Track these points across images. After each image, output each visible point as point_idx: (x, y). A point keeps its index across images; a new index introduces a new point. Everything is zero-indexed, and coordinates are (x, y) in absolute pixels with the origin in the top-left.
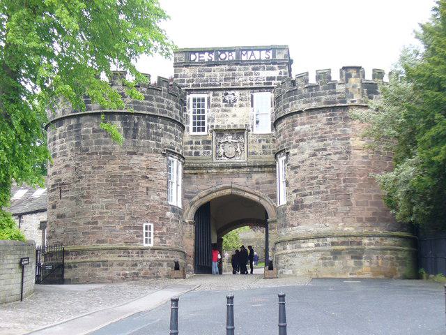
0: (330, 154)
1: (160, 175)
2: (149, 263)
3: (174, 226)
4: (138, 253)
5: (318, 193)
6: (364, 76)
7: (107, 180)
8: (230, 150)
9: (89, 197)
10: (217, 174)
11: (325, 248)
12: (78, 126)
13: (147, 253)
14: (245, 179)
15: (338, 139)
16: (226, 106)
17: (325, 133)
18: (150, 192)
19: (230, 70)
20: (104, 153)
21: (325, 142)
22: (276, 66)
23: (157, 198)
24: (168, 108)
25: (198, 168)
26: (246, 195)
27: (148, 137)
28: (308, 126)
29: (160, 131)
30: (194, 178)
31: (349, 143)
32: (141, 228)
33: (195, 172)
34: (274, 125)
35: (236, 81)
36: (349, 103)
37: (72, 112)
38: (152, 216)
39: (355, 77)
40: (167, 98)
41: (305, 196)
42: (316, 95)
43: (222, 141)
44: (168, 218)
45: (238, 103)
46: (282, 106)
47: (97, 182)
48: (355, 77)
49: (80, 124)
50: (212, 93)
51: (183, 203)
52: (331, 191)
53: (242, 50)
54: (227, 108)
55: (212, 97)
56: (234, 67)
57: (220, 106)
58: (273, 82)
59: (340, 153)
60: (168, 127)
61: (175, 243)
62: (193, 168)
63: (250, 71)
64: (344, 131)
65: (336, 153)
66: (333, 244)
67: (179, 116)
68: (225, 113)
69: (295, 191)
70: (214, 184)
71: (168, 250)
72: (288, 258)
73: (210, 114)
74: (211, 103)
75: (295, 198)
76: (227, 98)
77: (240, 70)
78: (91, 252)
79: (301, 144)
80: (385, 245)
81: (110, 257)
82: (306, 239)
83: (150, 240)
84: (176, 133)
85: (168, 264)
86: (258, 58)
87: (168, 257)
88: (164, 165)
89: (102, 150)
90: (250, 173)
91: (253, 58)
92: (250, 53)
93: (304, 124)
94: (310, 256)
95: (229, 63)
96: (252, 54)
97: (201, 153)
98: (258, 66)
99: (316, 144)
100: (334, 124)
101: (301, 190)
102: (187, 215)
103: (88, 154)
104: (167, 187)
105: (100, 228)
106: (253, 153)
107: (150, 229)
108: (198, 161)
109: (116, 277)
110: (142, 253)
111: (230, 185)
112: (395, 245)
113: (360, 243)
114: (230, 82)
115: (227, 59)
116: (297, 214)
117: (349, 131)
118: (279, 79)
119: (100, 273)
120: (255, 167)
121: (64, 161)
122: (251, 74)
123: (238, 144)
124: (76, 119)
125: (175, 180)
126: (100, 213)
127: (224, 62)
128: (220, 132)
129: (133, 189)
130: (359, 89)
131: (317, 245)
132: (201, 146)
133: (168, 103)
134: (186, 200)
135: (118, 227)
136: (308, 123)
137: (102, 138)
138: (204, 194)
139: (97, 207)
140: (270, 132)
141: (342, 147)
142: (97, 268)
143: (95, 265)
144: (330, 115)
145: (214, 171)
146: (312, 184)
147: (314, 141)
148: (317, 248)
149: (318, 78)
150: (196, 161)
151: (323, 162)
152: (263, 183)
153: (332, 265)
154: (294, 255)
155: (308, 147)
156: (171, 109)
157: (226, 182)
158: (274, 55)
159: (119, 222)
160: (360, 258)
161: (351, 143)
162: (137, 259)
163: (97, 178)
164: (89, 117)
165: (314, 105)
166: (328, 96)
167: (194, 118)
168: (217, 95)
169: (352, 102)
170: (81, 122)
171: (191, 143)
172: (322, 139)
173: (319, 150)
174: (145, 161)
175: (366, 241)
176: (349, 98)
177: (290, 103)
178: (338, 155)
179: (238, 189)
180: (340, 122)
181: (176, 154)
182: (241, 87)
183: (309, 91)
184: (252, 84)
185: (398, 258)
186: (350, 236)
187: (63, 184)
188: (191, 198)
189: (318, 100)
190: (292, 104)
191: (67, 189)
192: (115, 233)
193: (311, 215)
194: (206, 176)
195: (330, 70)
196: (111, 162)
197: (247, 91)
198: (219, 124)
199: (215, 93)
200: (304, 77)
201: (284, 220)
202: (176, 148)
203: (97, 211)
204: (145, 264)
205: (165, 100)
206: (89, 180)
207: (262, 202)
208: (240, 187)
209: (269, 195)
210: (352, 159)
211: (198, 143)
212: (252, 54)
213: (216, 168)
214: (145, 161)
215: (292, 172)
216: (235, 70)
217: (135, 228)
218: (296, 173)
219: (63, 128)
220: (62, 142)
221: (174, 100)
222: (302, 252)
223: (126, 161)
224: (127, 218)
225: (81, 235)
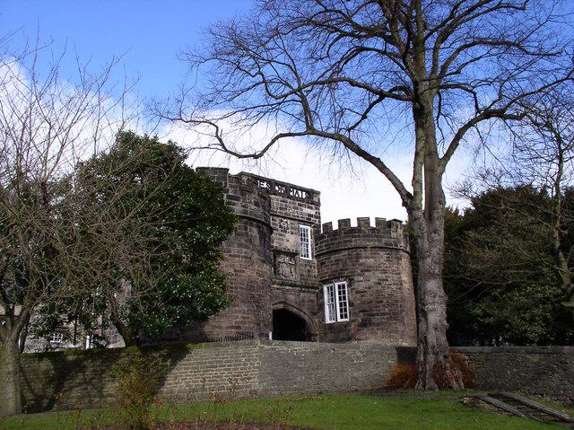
5: (384, 314)
20: (246, 257)
45: (289, 230)
56: (286, 199)
79: (366, 273)
103: (230, 256)
212: (297, 192)
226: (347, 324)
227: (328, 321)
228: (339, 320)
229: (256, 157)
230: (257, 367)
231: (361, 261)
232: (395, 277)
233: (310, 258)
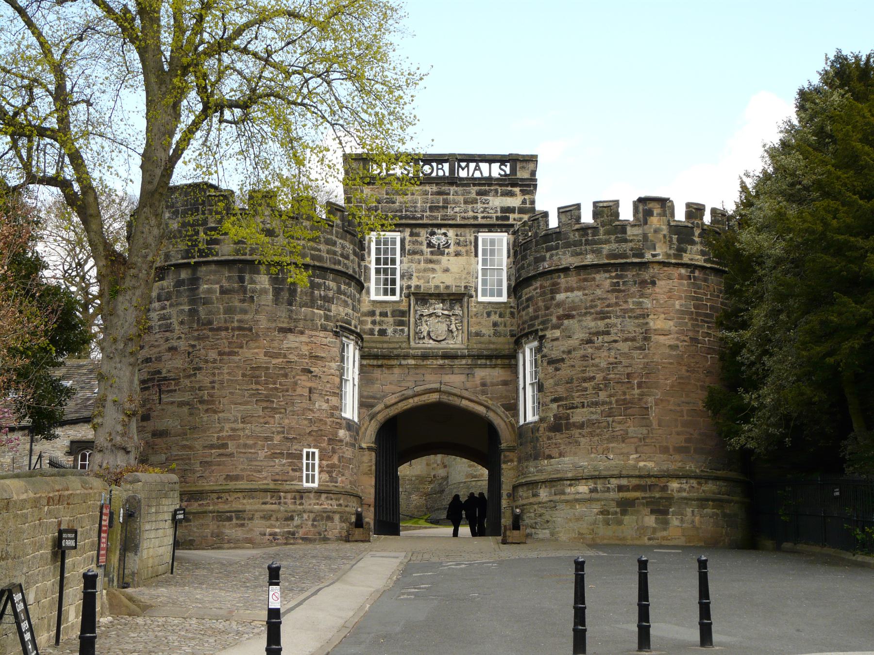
0: (615, 341)
1: (330, 368)
2: (312, 516)
3: (348, 453)
4: (295, 498)
5: (596, 404)
6: (673, 214)
7: (244, 375)
8: (441, 328)
9: (212, 402)
10: (417, 367)
11: (607, 494)
12: (194, 281)
13: (309, 498)
14: (462, 378)
15: (630, 317)
16: (432, 253)
17: (608, 306)
18: (315, 396)
19: (439, 193)
20: (240, 329)
21: (607, 321)
22: (517, 190)
23: (325, 406)
24: (342, 255)
25: (384, 357)
26: (465, 403)
27: (312, 304)
28: (580, 293)
29: (330, 294)
30: (377, 373)
31: (647, 323)
32: (300, 457)
33: (380, 362)
34: (515, 290)
35: (450, 212)
36: (648, 257)
37: (183, 258)
38: (316, 437)
39: (659, 215)
40: (341, 238)
41: (573, 408)
42: (595, 242)
43: (426, 312)
44: (341, 441)
45: (452, 249)
46: (531, 258)
47: (227, 377)
48: (659, 215)
49: (198, 279)
50: (408, 231)
51: (359, 417)
52: (617, 401)
53: (463, 161)
54: (434, 257)
55: (408, 238)
56: (445, 188)
57: (421, 253)
58: (512, 216)
59: (633, 340)
60: (343, 287)
61: (350, 482)
62: (376, 357)
63: (474, 195)
64: (640, 303)
65: (626, 340)
66: (620, 488)
67: (357, 269)
68: (431, 266)
69: (555, 400)
70: (411, 384)
71: (340, 493)
72: (543, 511)
73: (406, 266)
74: (407, 247)
75: (555, 412)
76: (434, 240)
77: (456, 193)
78: (215, 496)
79: (566, 322)
80: (704, 491)
81: (249, 505)
82: (576, 480)
83: (313, 476)
84: (353, 300)
85: (341, 518)
86: (486, 174)
87: (340, 505)
88: (335, 351)
89: (236, 324)
90: (471, 367)
91: (477, 174)
92: (472, 165)
94: (579, 509)
95: (439, 181)
96: (477, 168)
97: (390, 331)
98: (487, 188)
99: (592, 324)
100: (624, 291)
101: (566, 399)
102: (365, 433)
103: (211, 330)
104: (340, 387)
105: (231, 455)
106: (477, 334)
107: (313, 459)
108: (385, 345)
109: (258, 539)
110: (302, 498)
111: (436, 386)
112: (719, 494)
113: (664, 488)
114: (439, 215)
115: (434, 174)
116: (559, 438)
117: (647, 303)
118: (522, 211)
119: (231, 531)
120: (480, 357)
121: (167, 340)
122: (475, 201)
123: (453, 318)
124: (190, 271)
125: (350, 378)
126: (233, 430)
127: (429, 180)
128: (423, 298)
129: (287, 391)
130: (665, 236)
131: (593, 491)
132: (390, 319)
133: (343, 247)
134: (364, 410)
135: (262, 454)
136: (579, 289)
137: (237, 304)
138: (393, 401)
139: (227, 420)
140: (504, 298)
141: (637, 329)
142: (227, 523)
143: (223, 517)
144: (617, 277)
145: (412, 362)
146: (586, 389)
147: (589, 318)
148: (594, 495)
149: (596, 215)
150: (379, 345)
151: (606, 354)
152: (493, 385)
153: (620, 523)
154: (553, 505)
156: (347, 257)
157: (432, 380)
158: (513, 170)
159: (263, 446)
160: (665, 512)
161: (651, 324)
162: (292, 507)
163: (226, 371)
164: (213, 267)
165: (590, 259)
166: (614, 246)
167: (378, 271)
168: (418, 235)
169: (654, 256)
170: (199, 274)
171: (372, 313)
172: (603, 316)
173: (598, 334)
174: (307, 344)
175: (674, 485)
176: (649, 249)
177: (548, 255)
178: (630, 343)
180: (634, 289)
181: (352, 332)
182: (459, 221)
183: (583, 236)
184: (476, 218)
185: (725, 515)
186: (649, 476)
187: (165, 379)
188: (372, 406)
189: (598, 252)
190: (552, 256)
191: (173, 388)
192: (257, 463)
194: (396, 371)
195: (617, 203)
197: (467, 230)
198: (421, 283)
199: (415, 231)
200: (570, 212)
201: (535, 448)
202: (353, 322)
203: (227, 426)
204: (305, 516)
205: (339, 241)
206: (214, 374)
207: (491, 416)
209: (503, 405)
210: (653, 350)
211: (384, 314)
213: (414, 357)
214: (307, 344)
215: (551, 369)
216: (448, 194)
217: (290, 455)
218: (557, 369)
219: (164, 283)
220: (163, 308)
221: (351, 242)
222: (567, 501)
223: (275, 344)
224: (277, 439)
225: (198, 467)
226: (534, 428)
227: (522, 422)
228: (530, 418)
232: (631, 326)
233: (504, 298)
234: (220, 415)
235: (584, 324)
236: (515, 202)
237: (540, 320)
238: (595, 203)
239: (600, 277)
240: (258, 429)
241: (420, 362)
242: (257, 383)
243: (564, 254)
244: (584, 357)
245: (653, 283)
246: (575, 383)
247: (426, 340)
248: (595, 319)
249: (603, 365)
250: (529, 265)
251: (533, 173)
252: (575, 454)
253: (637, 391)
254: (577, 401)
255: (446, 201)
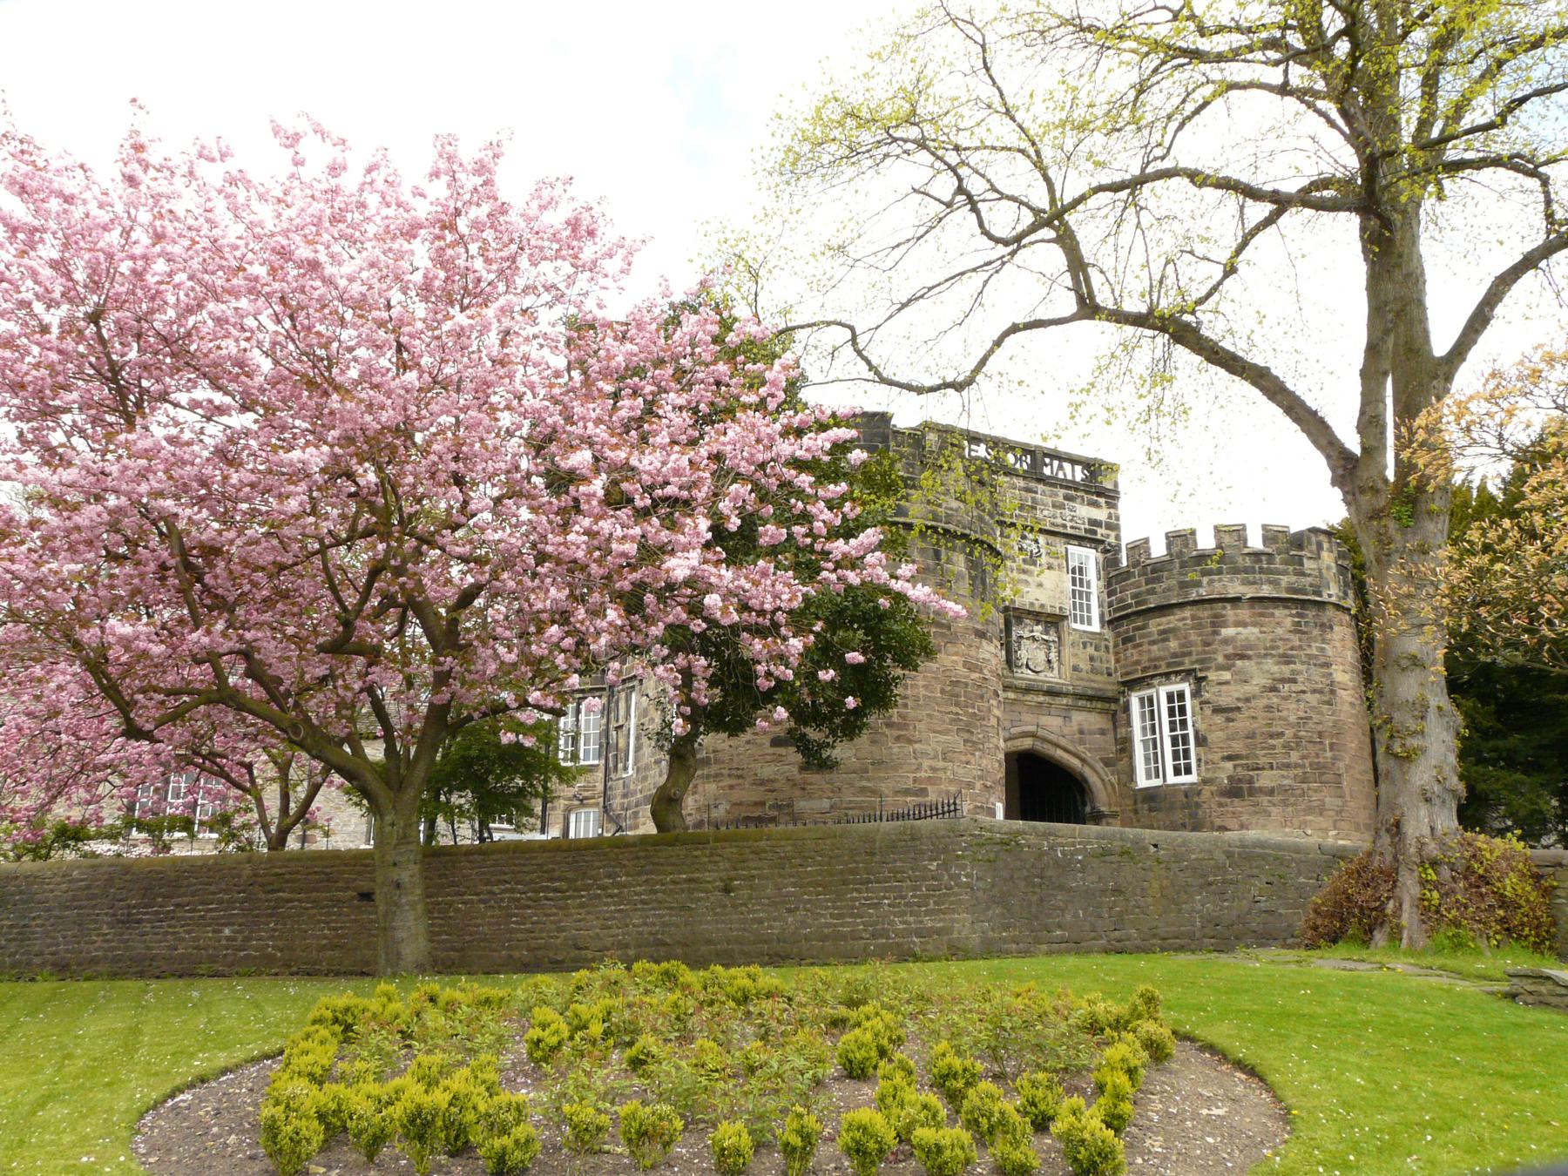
0: (1304, 692)
5: (1287, 766)
7: (943, 691)
17: (1292, 649)
19: (1028, 490)
22: (1102, 501)
26: (1059, 753)
28: (1256, 630)
36: (1325, 598)
45: (1044, 560)
53: (1046, 455)
56: (1033, 485)
59: (1321, 692)
63: (1061, 499)
65: (1314, 691)
68: (1023, 577)
69: (1230, 758)
75: (1231, 772)
77: (1044, 493)
79: (1239, 663)
90: (1069, 708)
91: (1061, 475)
92: (1056, 463)
93: (1244, 625)
99: (1275, 669)
111: (1032, 728)
122: (1062, 507)
126: (933, 769)
136: (1254, 625)
144: (1299, 615)
146: (1273, 747)
149: (1266, 540)
155: (1259, 673)
163: (921, 683)
165: (1266, 590)
166: (1294, 578)
172: (1287, 660)
173: (1283, 681)
177: (1205, 580)
179: (1045, 740)
190: (1211, 582)
193: (1274, 810)
196: (951, 648)
197: (1057, 540)
201: (1193, 815)
203: (926, 763)
207: (1087, 772)
208: (1051, 737)
212: (1061, 467)
215: (1219, 719)
218: (1229, 720)
226: (1190, 792)
227: (1142, 782)
228: (1172, 779)
229: (958, 387)
230: (968, 885)
231: (1228, 632)
232: (1316, 674)
233: (1096, 627)
234: (917, 746)
235: (1266, 667)
236: (1101, 514)
237: (1194, 657)
238: (1264, 527)
239: (1280, 613)
240: (961, 771)
241: (1020, 696)
242: (957, 704)
243: (1231, 580)
244: (1269, 708)
245: (1331, 628)
246: (1259, 739)
247: (1024, 669)
248: (1278, 663)
249: (1292, 719)
250: (1169, 589)
251: (1116, 484)
252: (1264, 827)
253: (1329, 754)
254: (1262, 761)
255: (1034, 500)
